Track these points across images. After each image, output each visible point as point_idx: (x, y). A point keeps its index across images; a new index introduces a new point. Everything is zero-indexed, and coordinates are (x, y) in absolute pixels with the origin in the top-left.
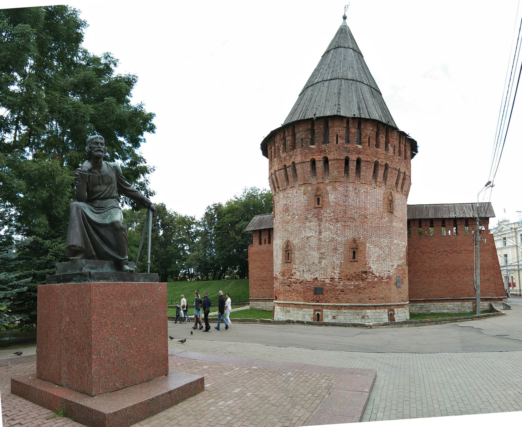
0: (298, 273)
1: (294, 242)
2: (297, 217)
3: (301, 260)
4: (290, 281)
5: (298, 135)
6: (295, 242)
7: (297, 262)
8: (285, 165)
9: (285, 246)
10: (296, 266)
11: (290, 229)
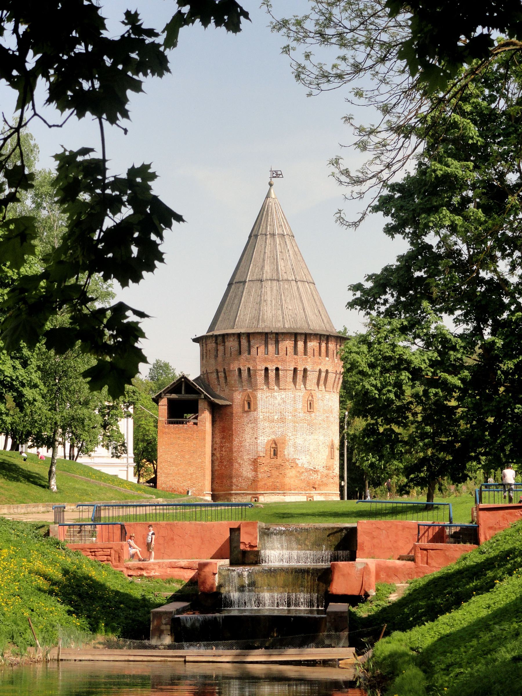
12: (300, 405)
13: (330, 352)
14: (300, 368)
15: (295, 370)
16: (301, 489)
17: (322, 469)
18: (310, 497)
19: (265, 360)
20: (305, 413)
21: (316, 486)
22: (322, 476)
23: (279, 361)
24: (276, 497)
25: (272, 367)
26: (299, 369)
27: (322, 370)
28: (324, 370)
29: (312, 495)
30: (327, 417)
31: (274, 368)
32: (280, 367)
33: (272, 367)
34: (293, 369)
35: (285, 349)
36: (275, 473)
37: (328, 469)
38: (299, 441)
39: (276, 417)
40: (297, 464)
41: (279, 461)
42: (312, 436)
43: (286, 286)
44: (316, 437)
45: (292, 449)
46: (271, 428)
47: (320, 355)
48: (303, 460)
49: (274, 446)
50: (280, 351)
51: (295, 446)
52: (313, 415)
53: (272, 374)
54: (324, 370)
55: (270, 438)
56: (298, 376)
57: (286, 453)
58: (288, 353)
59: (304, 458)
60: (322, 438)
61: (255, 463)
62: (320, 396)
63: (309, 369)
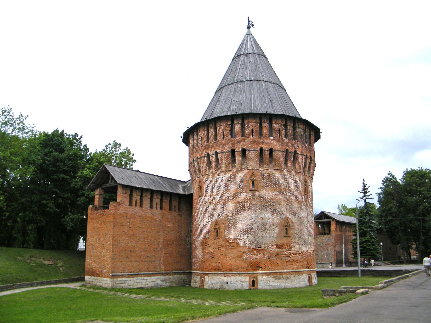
0: (297, 246)
1: (293, 220)
2: (294, 198)
3: (300, 235)
4: (290, 253)
5: (298, 130)
6: (295, 219)
7: (296, 237)
8: (287, 150)
9: (283, 222)
10: (296, 240)
11: (288, 207)
12: (241, 185)
13: (276, 131)
14: (238, 149)
15: (233, 152)
16: (243, 269)
17: (269, 248)
18: (254, 277)
19: (207, 147)
20: (246, 192)
21: (262, 266)
22: (271, 255)
23: (217, 145)
24: (218, 277)
25: (212, 152)
26: (237, 149)
27: (265, 149)
28: (266, 148)
29: (255, 275)
30: (277, 195)
31: (214, 152)
32: (218, 151)
33: (212, 152)
34: (229, 150)
35: (222, 133)
36: (218, 254)
37: (280, 248)
38: (241, 221)
39: (218, 199)
40: (239, 244)
41: (220, 242)
42: (256, 215)
43: (239, 86)
44: (261, 216)
45: (232, 229)
46: (214, 210)
47: (261, 134)
48: (245, 240)
49: (217, 227)
50: (218, 136)
51: (236, 225)
52: (256, 194)
53: (213, 159)
54: (266, 148)
55: (213, 220)
56: (237, 157)
57: (226, 233)
58: (225, 136)
59: (245, 237)
60: (270, 216)
61: (204, 245)
62: (266, 175)
63: (247, 148)
